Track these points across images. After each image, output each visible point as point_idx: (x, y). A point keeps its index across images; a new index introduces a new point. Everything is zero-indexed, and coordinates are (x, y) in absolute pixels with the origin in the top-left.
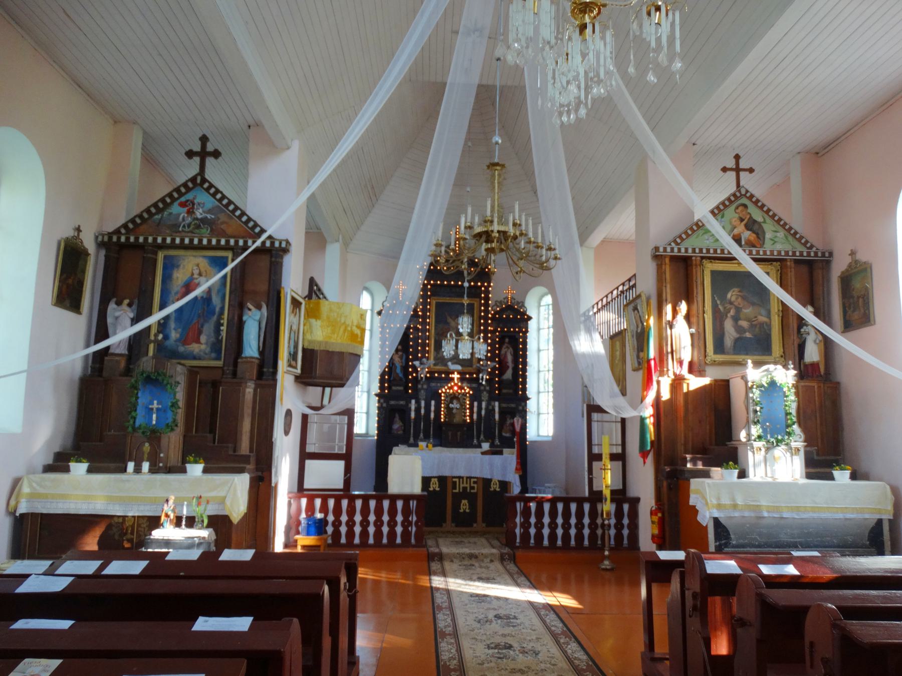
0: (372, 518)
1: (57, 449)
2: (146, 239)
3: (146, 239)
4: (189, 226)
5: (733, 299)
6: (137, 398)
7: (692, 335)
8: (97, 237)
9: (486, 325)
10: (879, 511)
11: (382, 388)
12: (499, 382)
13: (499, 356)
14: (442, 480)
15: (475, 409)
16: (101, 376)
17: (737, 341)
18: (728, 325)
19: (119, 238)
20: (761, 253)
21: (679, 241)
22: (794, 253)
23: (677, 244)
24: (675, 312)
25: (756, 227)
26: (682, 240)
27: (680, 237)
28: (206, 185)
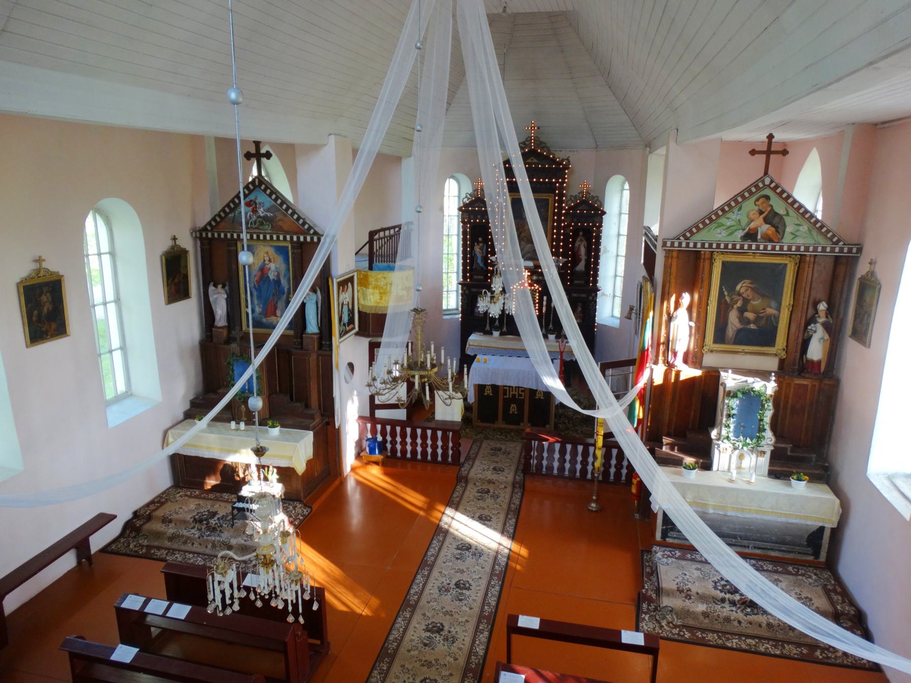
0: (419, 441)
1: (192, 397)
2: (226, 235)
3: (226, 235)
4: (255, 223)
5: (742, 290)
6: (233, 371)
7: (691, 327)
8: (192, 234)
9: (559, 221)
10: (823, 520)
11: (464, 277)
12: (571, 274)
13: (572, 249)
14: (495, 388)
15: (545, 303)
16: (212, 341)
17: (739, 331)
18: (733, 317)
19: (207, 235)
20: (777, 248)
21: (688, 235)
22: (815, 250)
23: (687, 238)
24: (677, 305)
25: (776, 221)
26: (692, 234)
27: (691, 231)
28: (263, 187)
